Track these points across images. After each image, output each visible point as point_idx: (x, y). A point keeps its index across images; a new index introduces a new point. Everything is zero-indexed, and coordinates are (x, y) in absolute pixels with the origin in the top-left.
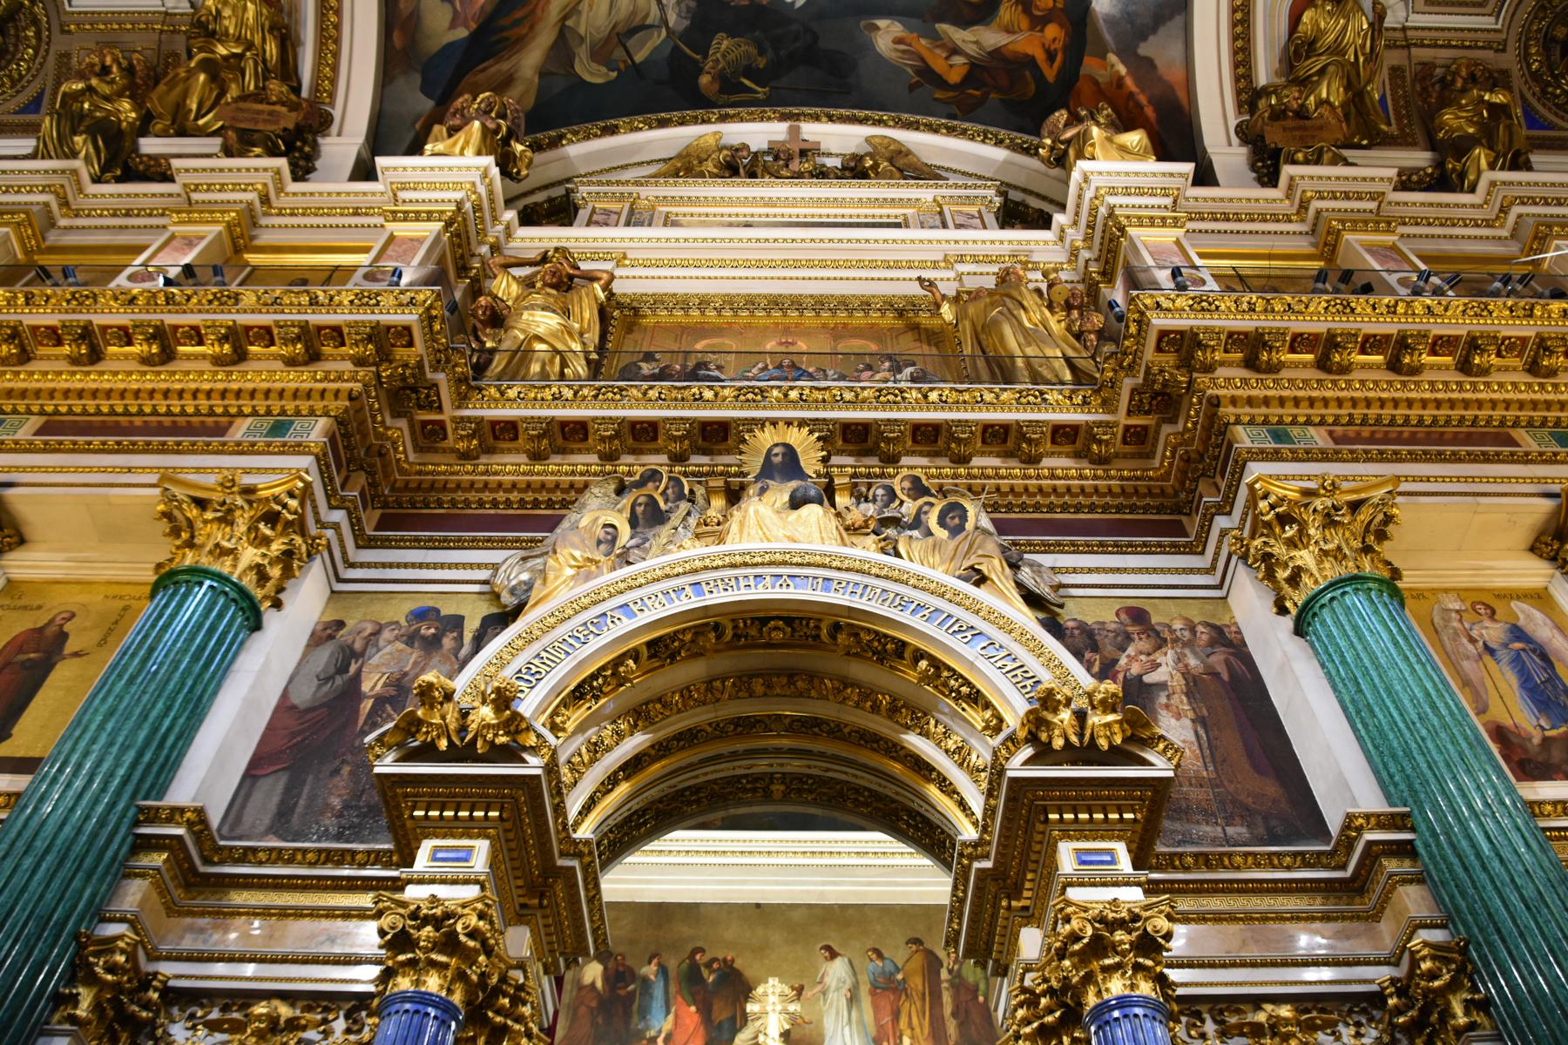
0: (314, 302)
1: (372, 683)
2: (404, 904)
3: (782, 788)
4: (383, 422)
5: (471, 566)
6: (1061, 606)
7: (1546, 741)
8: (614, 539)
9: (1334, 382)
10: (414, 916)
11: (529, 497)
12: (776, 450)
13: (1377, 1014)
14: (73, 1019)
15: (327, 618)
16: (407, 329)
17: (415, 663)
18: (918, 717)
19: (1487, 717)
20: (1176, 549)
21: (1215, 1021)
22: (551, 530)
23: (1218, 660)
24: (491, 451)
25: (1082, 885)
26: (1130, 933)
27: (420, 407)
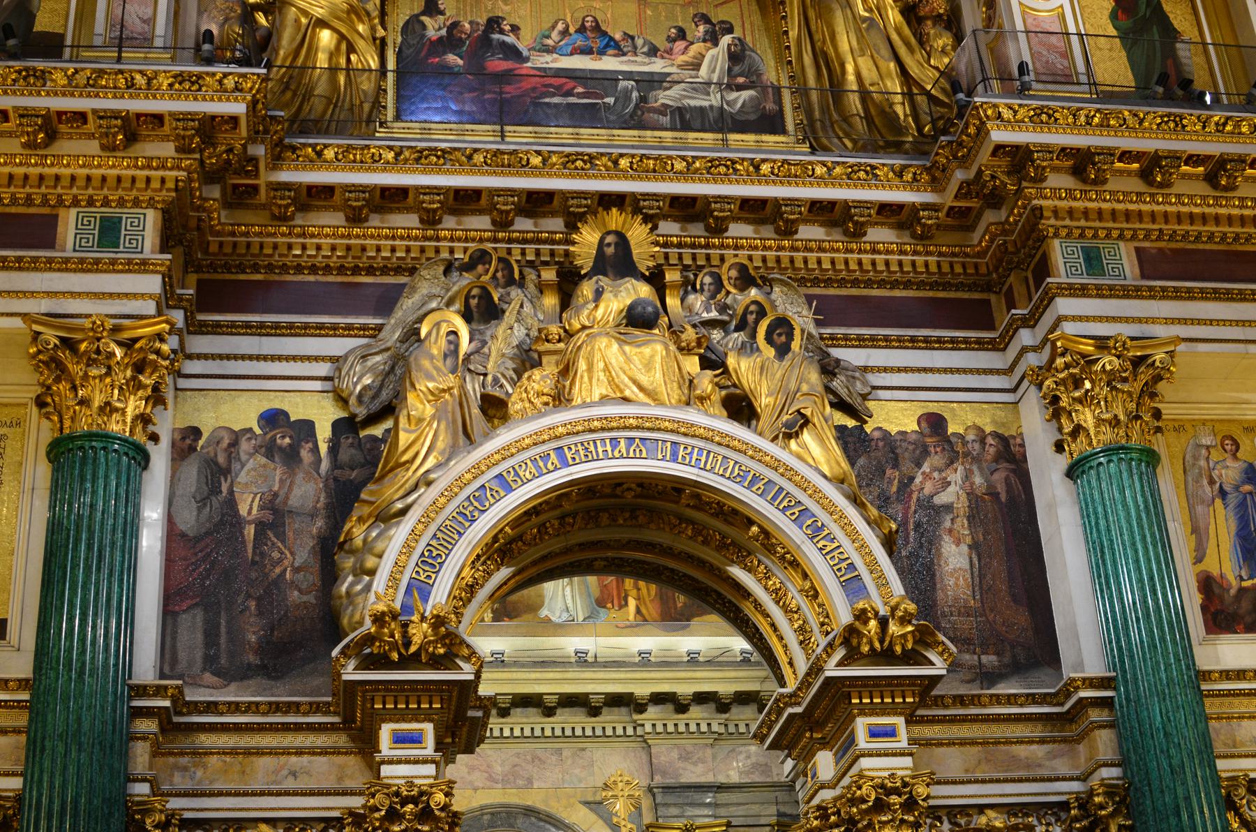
0: (131, 85)
1: (248, 506)
2: (389, 786)
5: (309, 358)
7: (1242, 590)
8: (457, 346)
9: (1152, 195)
10: (397, 794)
12: (609, 239)
13: (1063, 815)
16: (234, 120)
17: (281, 481)
18: (742, 554)
19: (1201, 567)
20: (981, 345)
21: (950, 823)
23: (999, 477)
24: (304, 208)
25: (871, 755)
26: (900, 796)
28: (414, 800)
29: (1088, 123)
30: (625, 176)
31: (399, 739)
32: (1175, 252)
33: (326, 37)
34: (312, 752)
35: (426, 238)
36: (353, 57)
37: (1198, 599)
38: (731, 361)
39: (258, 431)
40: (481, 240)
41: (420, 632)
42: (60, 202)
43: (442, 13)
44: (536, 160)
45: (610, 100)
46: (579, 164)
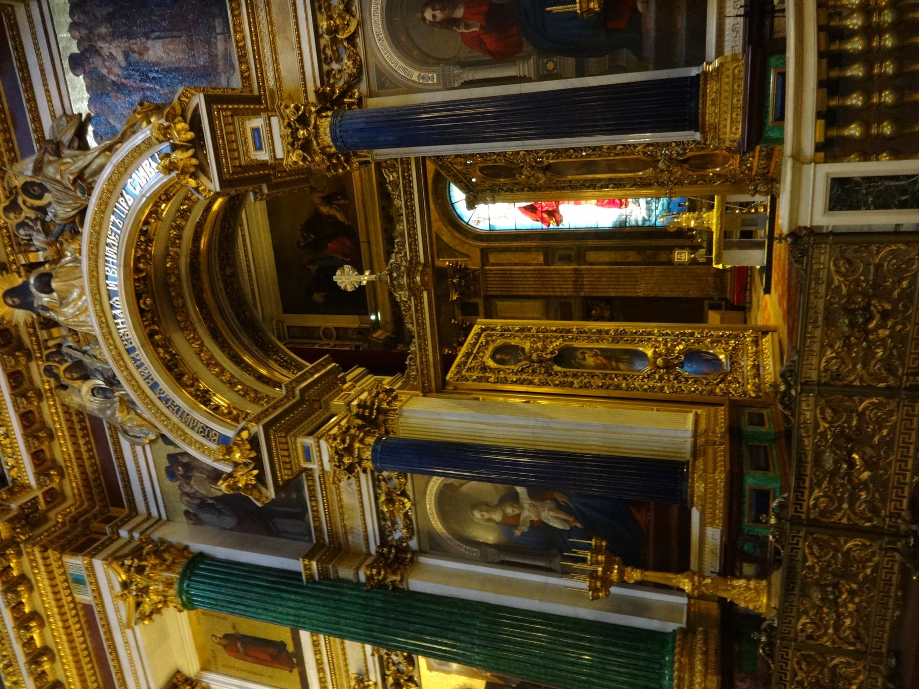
2: (335, 472)
3: (228, 269)
4: (54, 526)
6: (80, 115)
10: (339, 467)
11: (79, 434)
12: (10, 302)
14: (401, 581)
15: (184, 519)
17: (201, 473)
22: (101, 420)
24: (54, 460)
26: (297, 129)
27: (37, 509)
28: (341, 457)
31: (308, 458)
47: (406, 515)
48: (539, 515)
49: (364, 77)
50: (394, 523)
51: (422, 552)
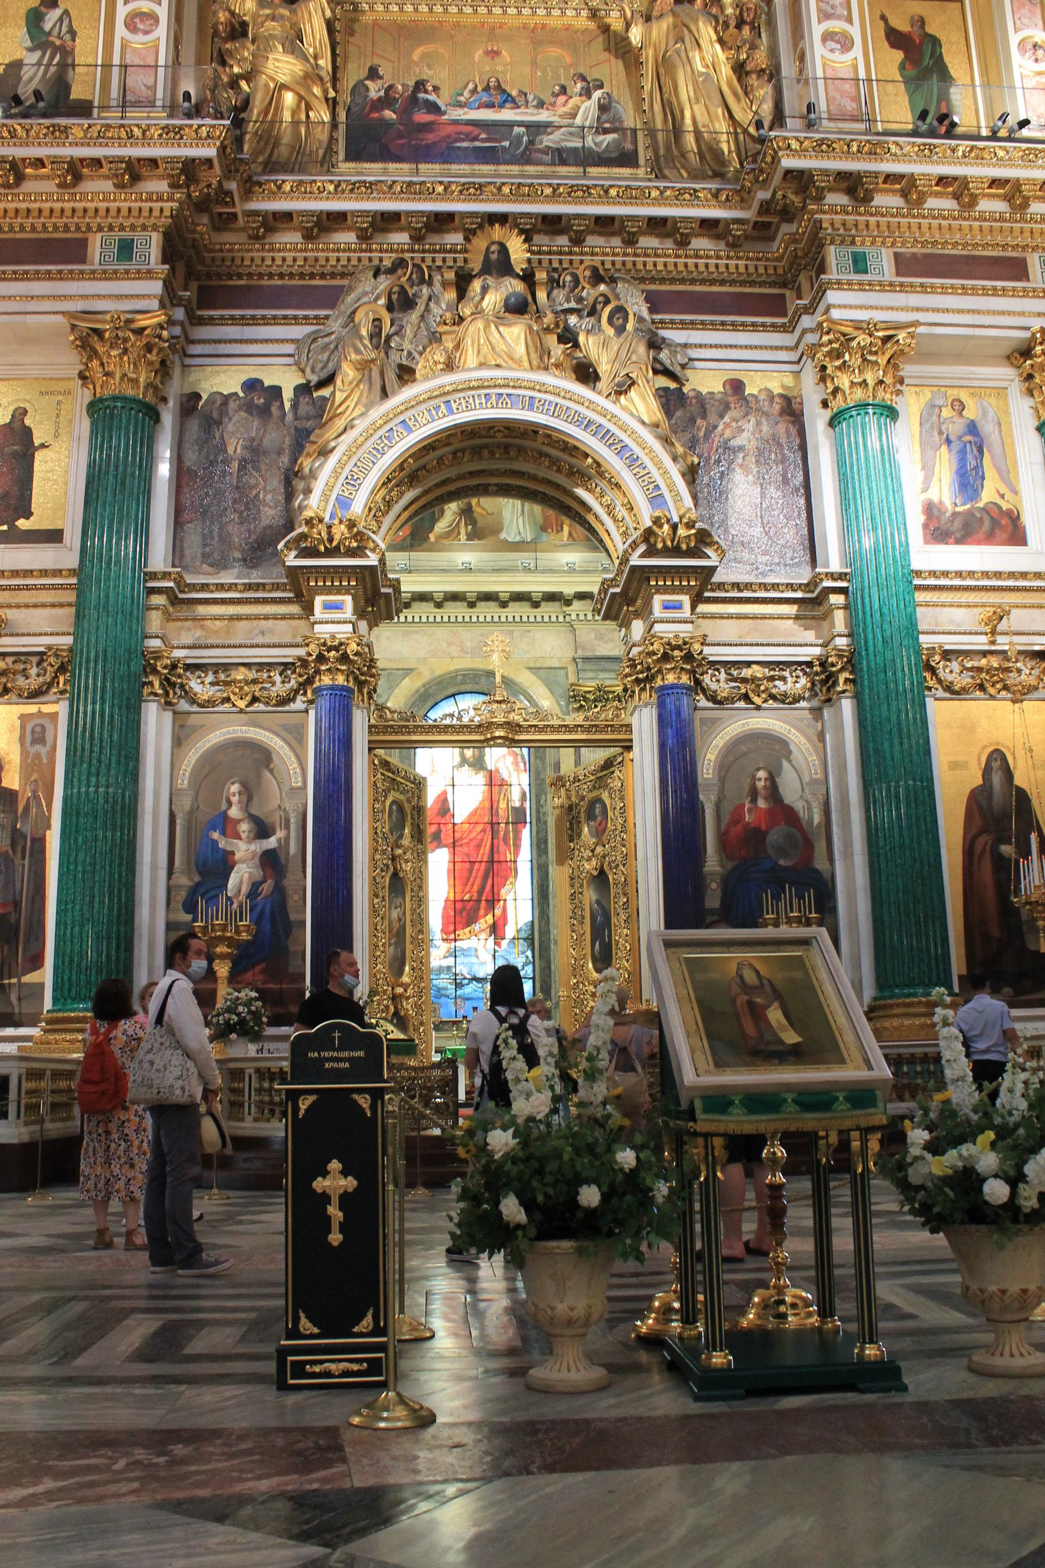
0: (130, 136)
1: (235, 447)
2: (319, 639)
7: (955, 514)
10: (324, 644)
11: (307, 269)
12: (494, 248)
16: (209, 161)
20: (775, 328)
25: (662, 622)
29: (858, 151)
30: (506, 199)
31: (327, 607)
32: (926, 256)
33: (289, 98)
34: (275, 617)
35: (362, 251)
36: (311, 114)
37: (922, 518)
38: (581, 339)
39: (241, 394)
40: (403, 251)
41: (340, 531)
42: (89, 228)
43: (381, 78)
44: (440, 189)
45: (506, 144)
46: (472, 191)
47: (228, 700)
48: (243, 862)
49: (710, 705)
50: (212, 684)
51: (175, 713)
